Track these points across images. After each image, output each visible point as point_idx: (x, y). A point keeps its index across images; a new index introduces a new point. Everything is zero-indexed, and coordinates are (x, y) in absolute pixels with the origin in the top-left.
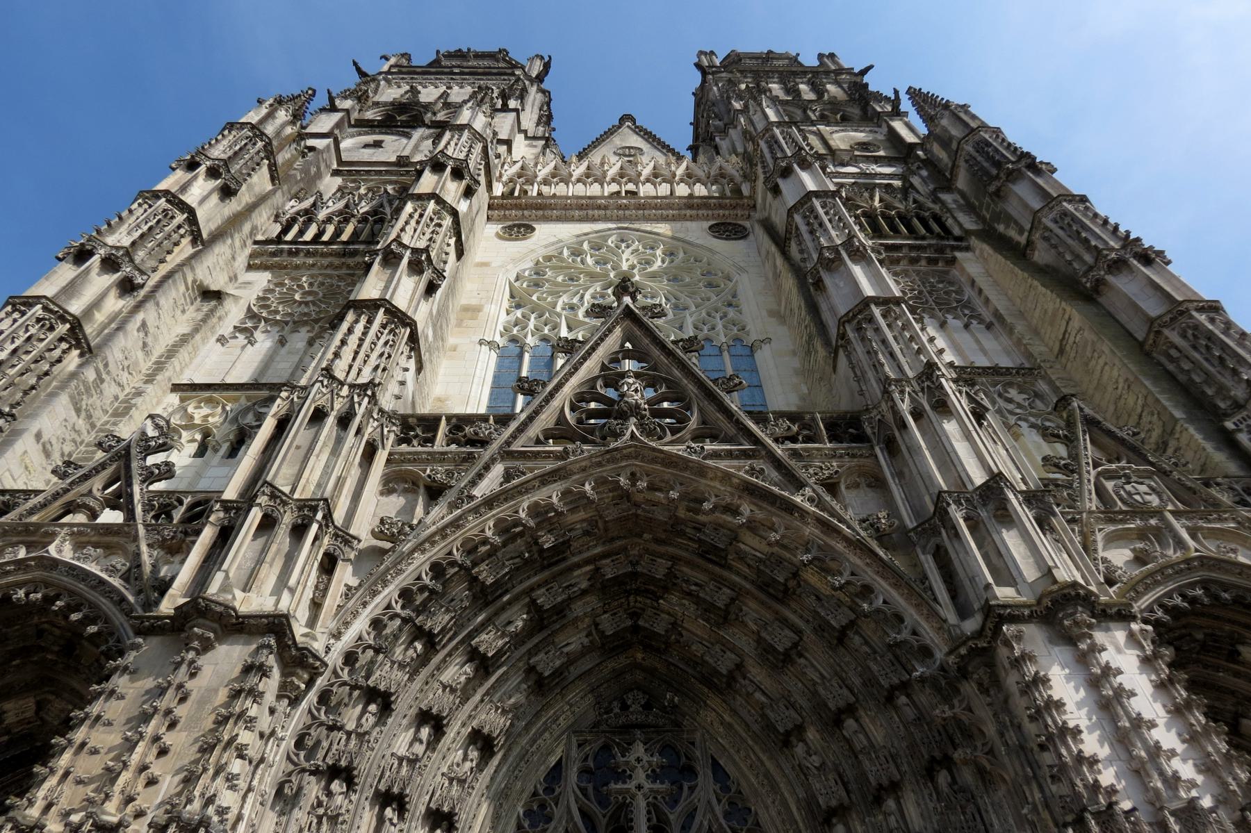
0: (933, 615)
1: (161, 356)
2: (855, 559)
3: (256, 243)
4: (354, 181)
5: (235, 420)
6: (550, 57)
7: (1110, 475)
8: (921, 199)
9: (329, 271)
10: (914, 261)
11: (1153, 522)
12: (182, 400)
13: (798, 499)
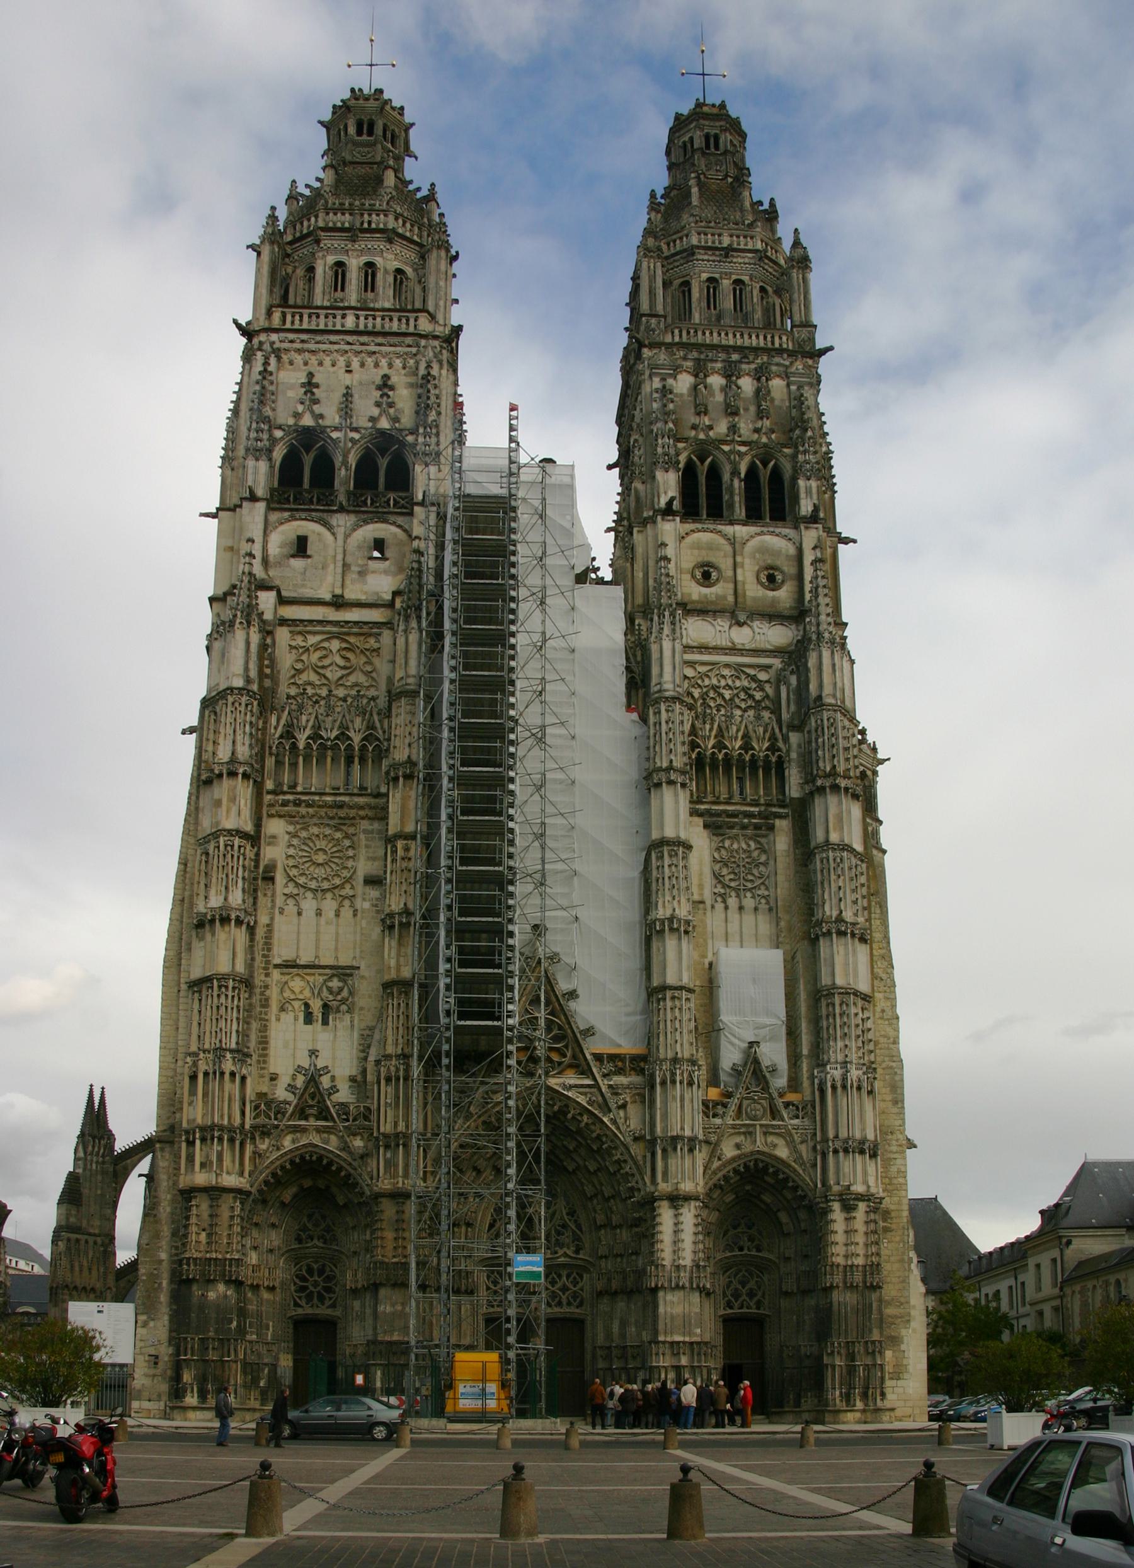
0: (643, 1179)
1: (263, 950)
2: (622, 1148)
3: (269, 793)
4: (300, 633)
5: (319, 993)
6: (457, 253)
7: (747, 1098)
8: (777, 730)
9: (326, 821)
10: (744, 827)
11: (751, 1129)
12: (282, 974)
13: (605, 1120)
